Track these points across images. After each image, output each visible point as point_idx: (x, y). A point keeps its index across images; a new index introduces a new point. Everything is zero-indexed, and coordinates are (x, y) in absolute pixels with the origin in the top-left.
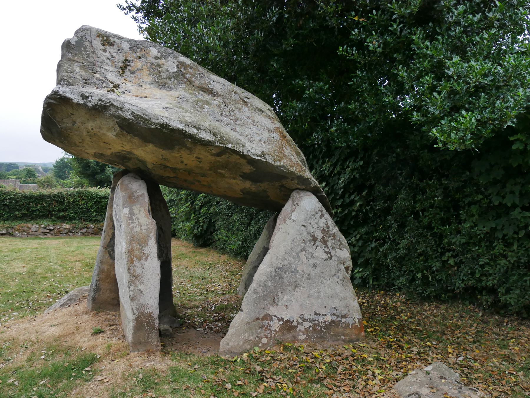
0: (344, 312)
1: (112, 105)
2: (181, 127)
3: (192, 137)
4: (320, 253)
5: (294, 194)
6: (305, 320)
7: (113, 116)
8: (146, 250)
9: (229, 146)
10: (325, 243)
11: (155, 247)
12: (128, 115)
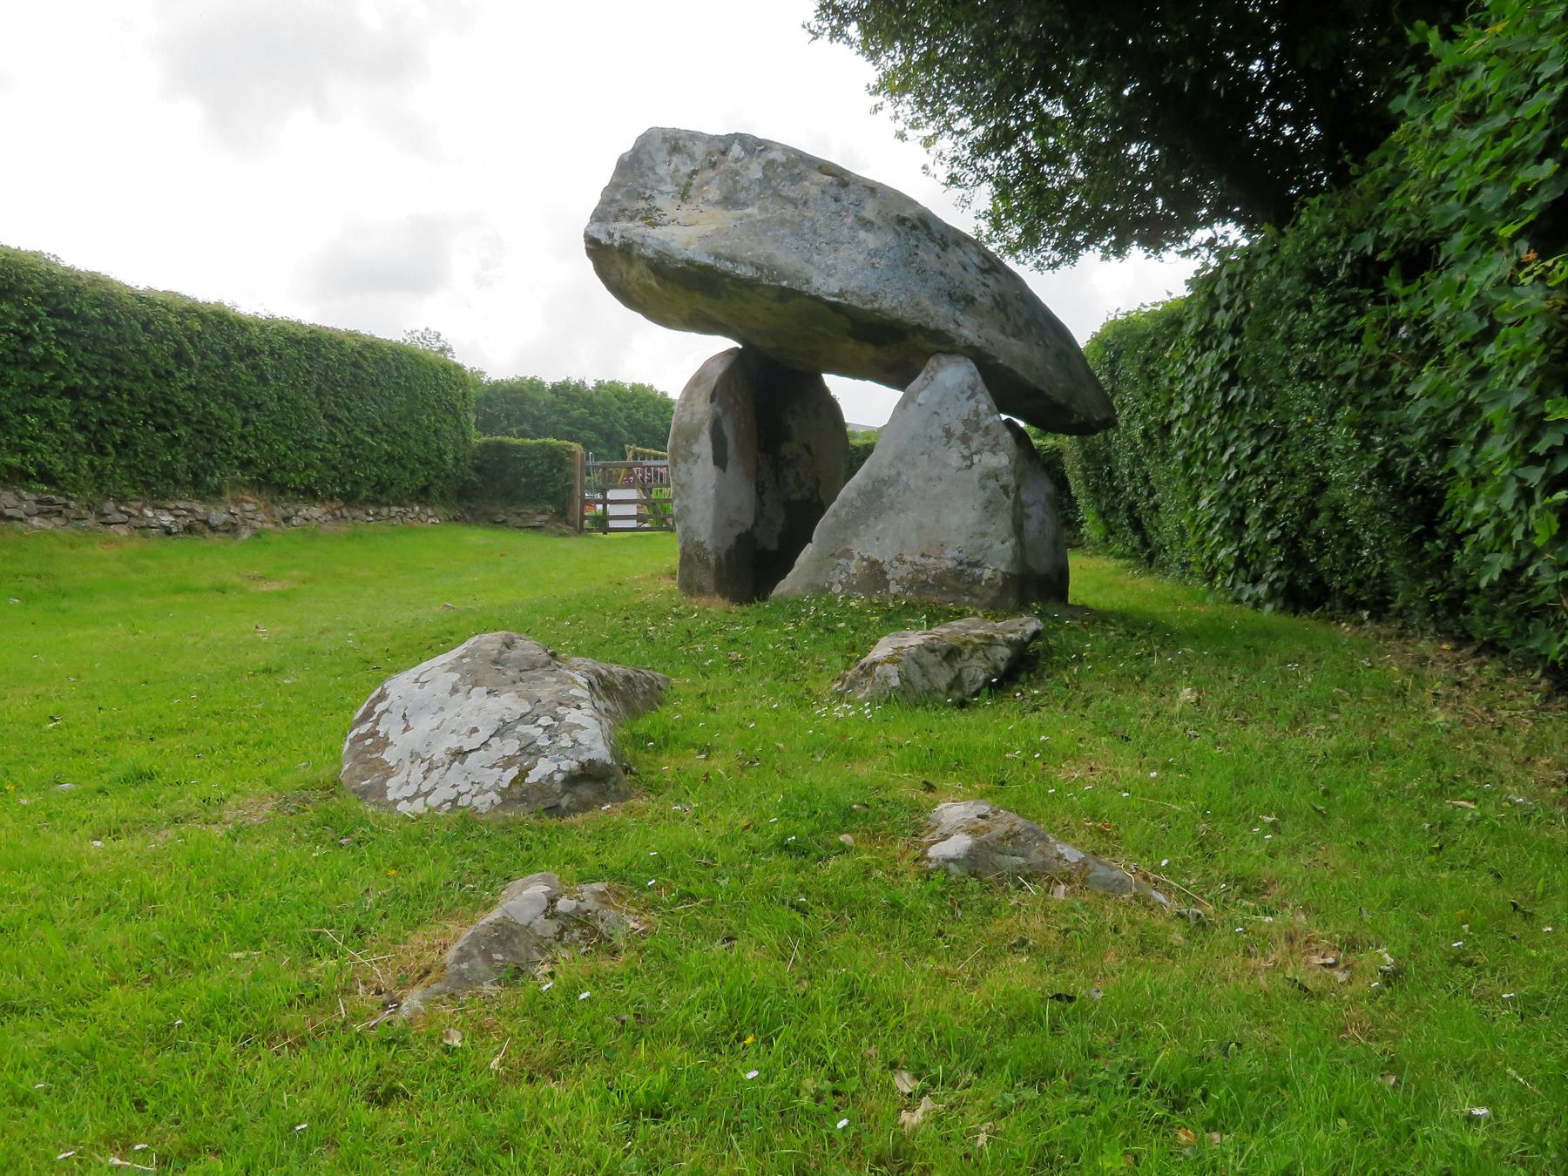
0: (978, 557)
2: (709, 261)
3: (726, 274)
4: (954, 457)
5: (932, 362)
8: (695, 449)
9: (784, 283)
10: (965, 440)
11: (710, 444)
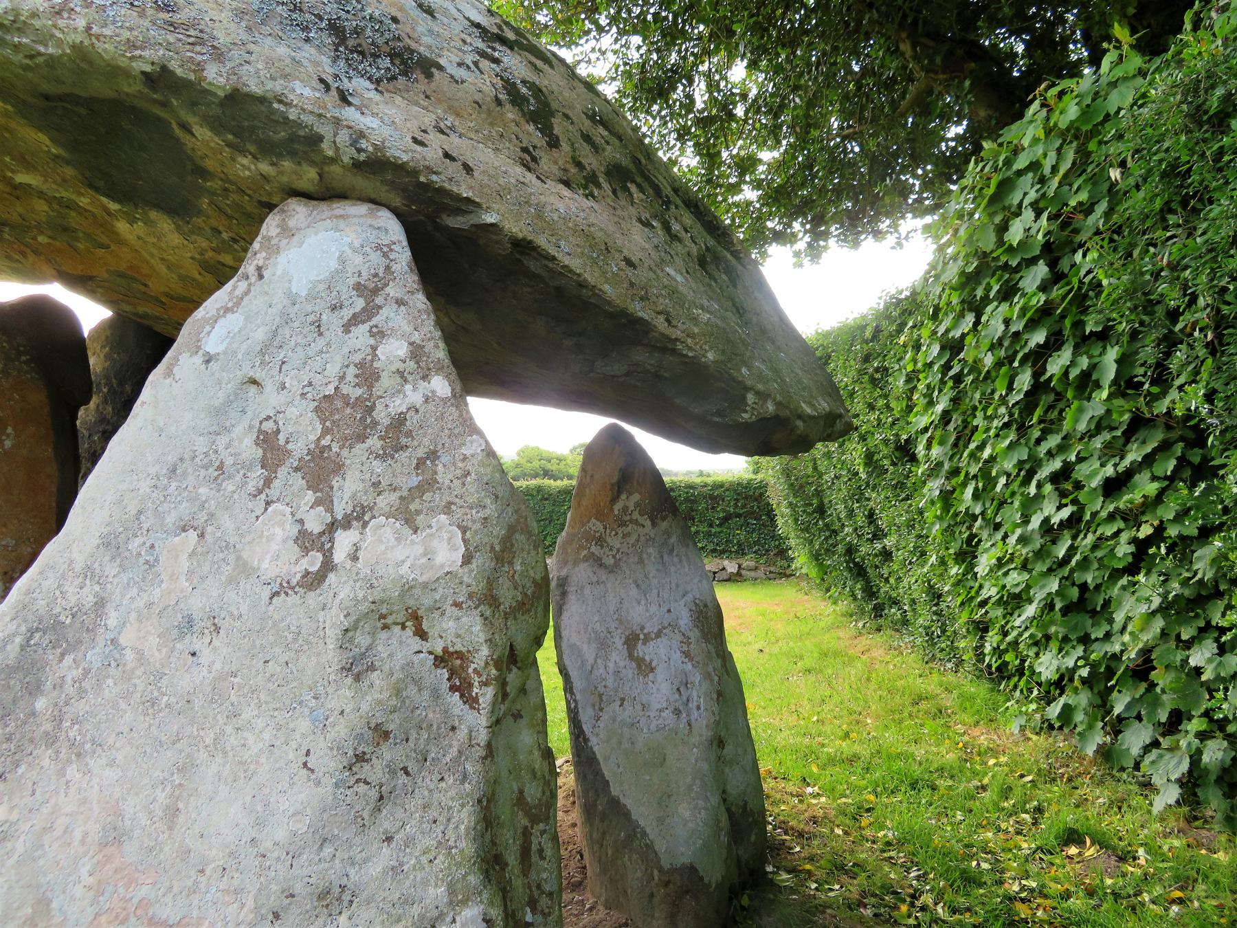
10: (320, 471)
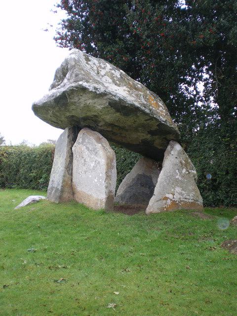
1: (111, 94)
2: (139, 106)
5: (171, 142)
6: (181, 201)
7: (109, 99)
12: (117, 99)
